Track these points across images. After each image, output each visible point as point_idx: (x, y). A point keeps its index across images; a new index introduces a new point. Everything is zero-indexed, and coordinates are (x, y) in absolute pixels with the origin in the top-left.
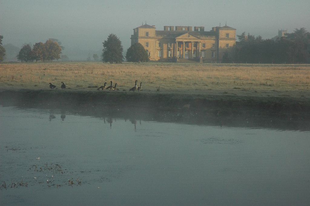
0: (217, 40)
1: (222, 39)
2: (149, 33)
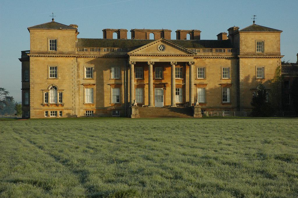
0: (236, 58)
1: (248, 56)
2: (60, 43)
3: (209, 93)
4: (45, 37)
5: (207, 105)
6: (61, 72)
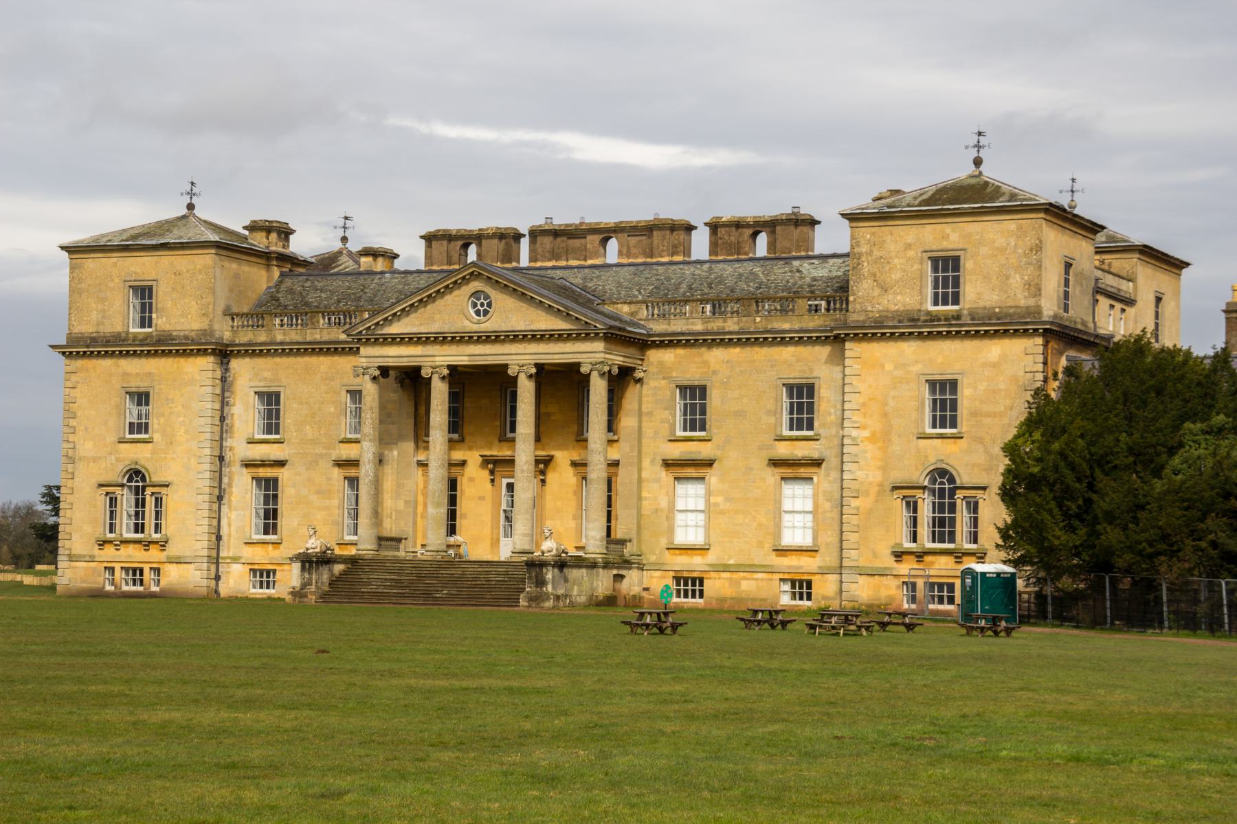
1: (883, 330)
2: (162, 297)
3: (720, 499)
4: (117, 280)
5: (711, 557)
6: (162, 415)
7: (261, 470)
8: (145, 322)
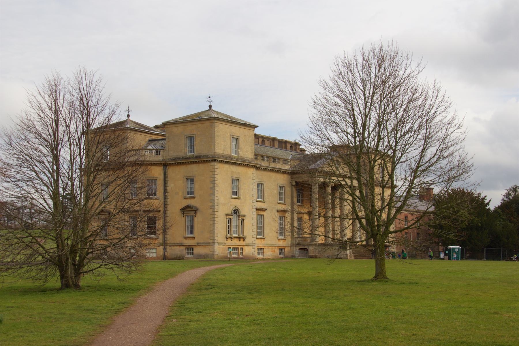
7: (260, 212)
8: (237, 152)
